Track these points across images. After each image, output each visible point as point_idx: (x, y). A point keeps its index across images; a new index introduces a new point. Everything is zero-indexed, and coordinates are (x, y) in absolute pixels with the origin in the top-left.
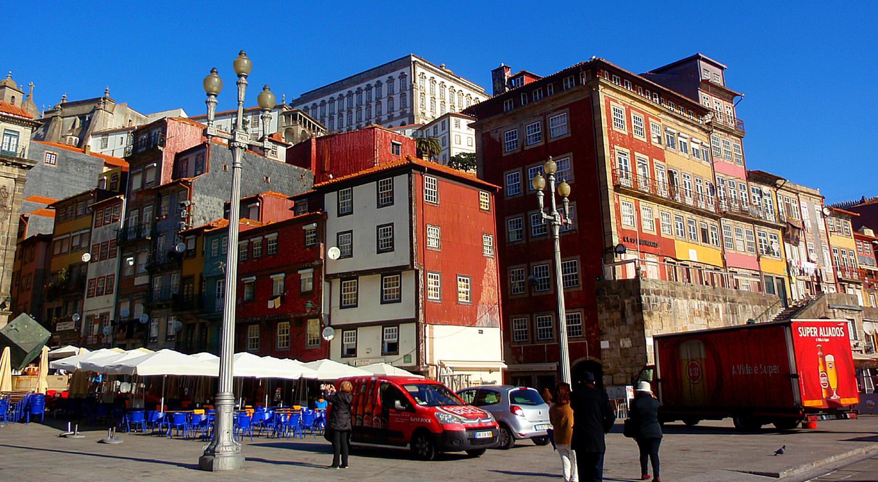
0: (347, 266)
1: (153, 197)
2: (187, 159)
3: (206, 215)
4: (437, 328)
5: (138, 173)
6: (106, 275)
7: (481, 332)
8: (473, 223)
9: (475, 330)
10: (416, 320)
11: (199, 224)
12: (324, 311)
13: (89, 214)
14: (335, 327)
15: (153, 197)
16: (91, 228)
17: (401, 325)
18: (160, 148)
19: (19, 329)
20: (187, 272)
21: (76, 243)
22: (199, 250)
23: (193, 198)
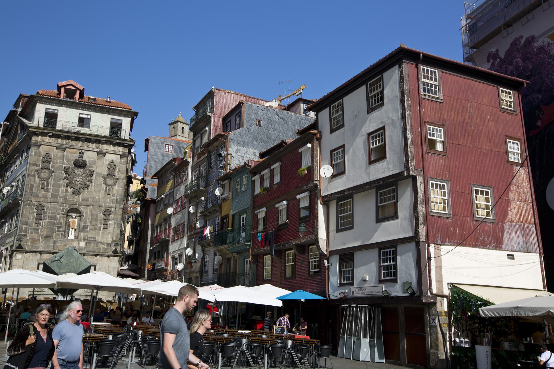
0: (340, 185)
1: (206, 155)
2: (230, 121)
4: (445, 249)
7: (511, 257)
8: (492, 124)
9: (505, 253)
10: (414, 239)
15: (206, 155)
16: (174, 189)
17: (400, 248)
18: (210, 114)
20: (224, 213)
23: (230, 149)
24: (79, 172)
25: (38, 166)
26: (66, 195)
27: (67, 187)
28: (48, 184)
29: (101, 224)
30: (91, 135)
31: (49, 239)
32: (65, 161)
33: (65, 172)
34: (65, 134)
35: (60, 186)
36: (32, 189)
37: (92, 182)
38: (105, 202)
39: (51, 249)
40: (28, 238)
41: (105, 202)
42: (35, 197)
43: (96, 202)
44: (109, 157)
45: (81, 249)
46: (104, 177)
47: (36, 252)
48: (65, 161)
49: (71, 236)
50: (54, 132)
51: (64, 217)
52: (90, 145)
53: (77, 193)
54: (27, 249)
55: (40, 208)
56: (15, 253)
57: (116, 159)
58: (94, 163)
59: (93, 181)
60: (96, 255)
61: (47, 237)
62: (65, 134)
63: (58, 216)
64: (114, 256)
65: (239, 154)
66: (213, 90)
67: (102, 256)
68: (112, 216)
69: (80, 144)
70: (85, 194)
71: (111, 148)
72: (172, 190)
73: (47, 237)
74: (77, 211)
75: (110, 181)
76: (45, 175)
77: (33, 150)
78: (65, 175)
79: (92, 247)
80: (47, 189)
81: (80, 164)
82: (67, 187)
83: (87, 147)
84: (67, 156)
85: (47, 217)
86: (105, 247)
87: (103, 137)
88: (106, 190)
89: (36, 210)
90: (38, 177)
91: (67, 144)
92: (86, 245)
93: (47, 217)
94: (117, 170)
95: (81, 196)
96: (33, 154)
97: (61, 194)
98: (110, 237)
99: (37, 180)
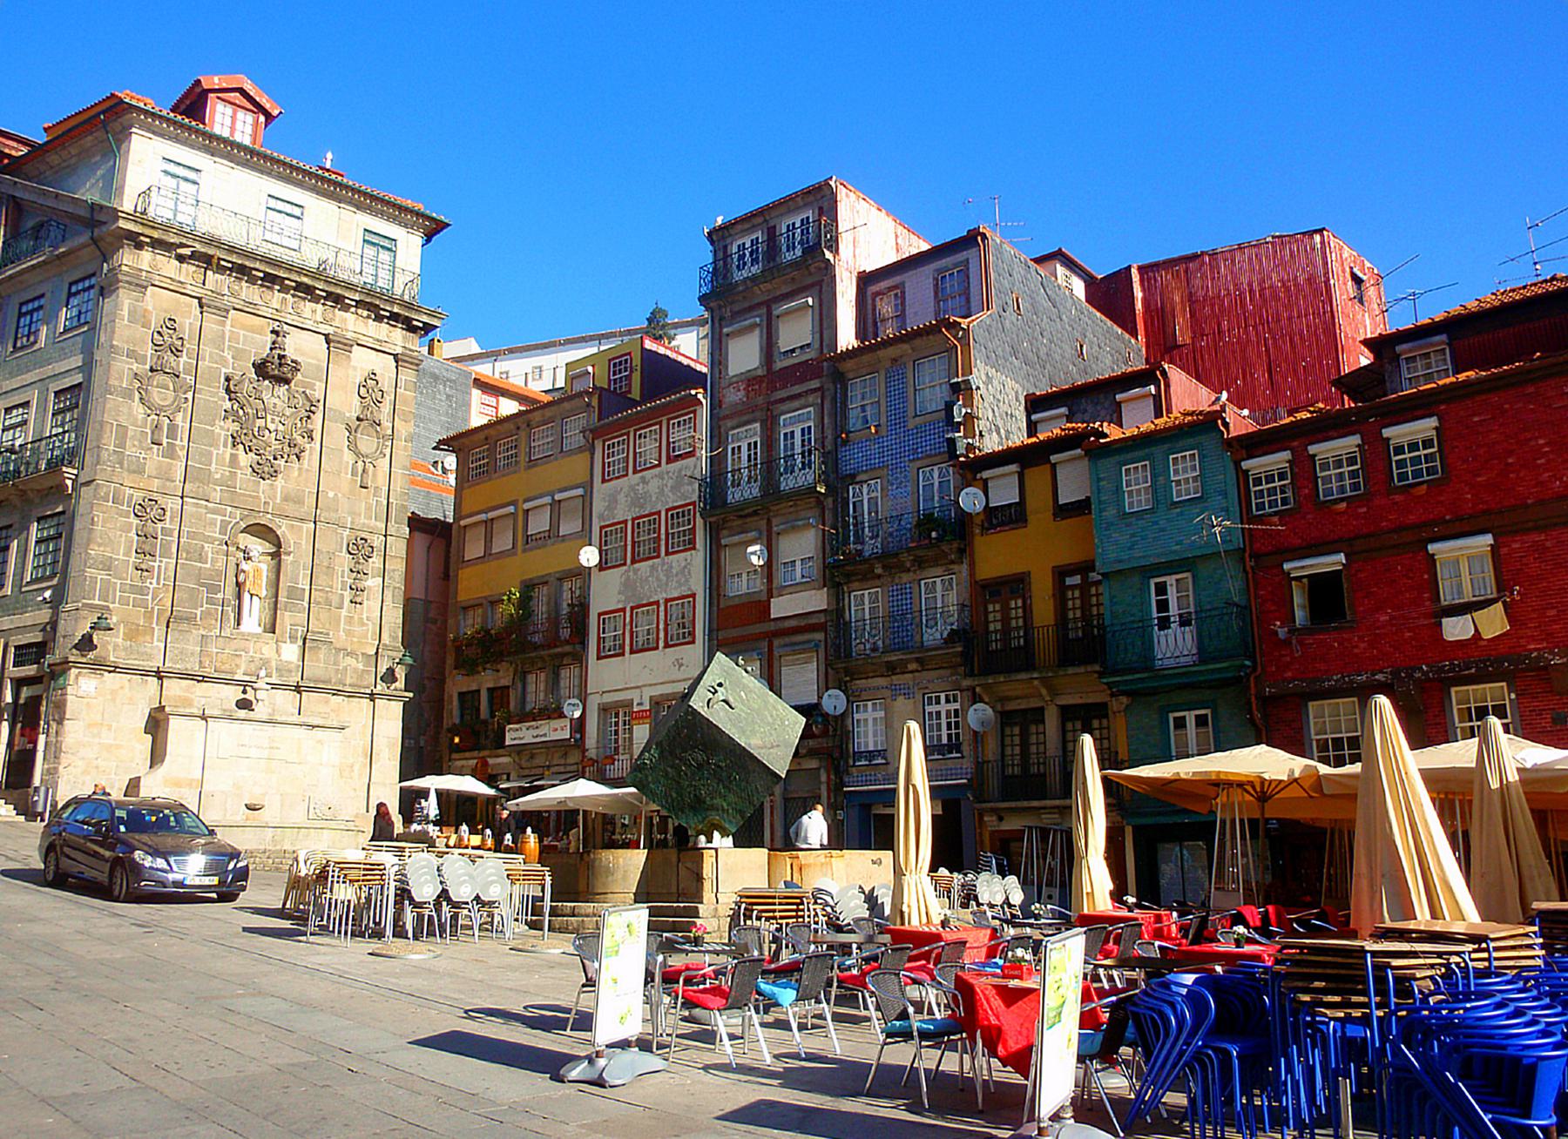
1: (815, 384)
2: (903, 284)
3: (1000, 423)
5: (755, 325)
6: (661, 597)
11: (991, 444)
13: (580, 450)
15: (815, 384)
21: (539, 523)
22: (1039, 504)
24: (275, 396)
25: (140, 359)
28: (173, 430)
31: (184, 626)
32: (228, 355)
33: (228, 391)
38: (354, 513)
39: (194, 668)
40: (115, 619)
41: (354, 513)
42: (131, 472)
43: (328, 509)
44: (363, 361)
47: (145, 673)
50: (198, 247)
52: (308, 307)
55: (147, 510)
56: (74, 671)
57: (384, 366)
59: (317, 436)
60: (337, 692)
64: (390, 697)
66: (832, 183)
67: (351, 695)
68: (376, 561)
69: (276, 298)
70: (294, 478)
74: (263, 531)
75: (367, 443)
76: (162, 394)
77: (125, 300)
78: (228, 405)
79: (318, 666)
81: (275, 370)
84: (234, 338)
87: (350, 287)
89: (136, 521)
94: (386, 408)
95: (280, 482)
96: (126, 313)
97: (218, 471)
98: (372, 628)
99: (139, 410)
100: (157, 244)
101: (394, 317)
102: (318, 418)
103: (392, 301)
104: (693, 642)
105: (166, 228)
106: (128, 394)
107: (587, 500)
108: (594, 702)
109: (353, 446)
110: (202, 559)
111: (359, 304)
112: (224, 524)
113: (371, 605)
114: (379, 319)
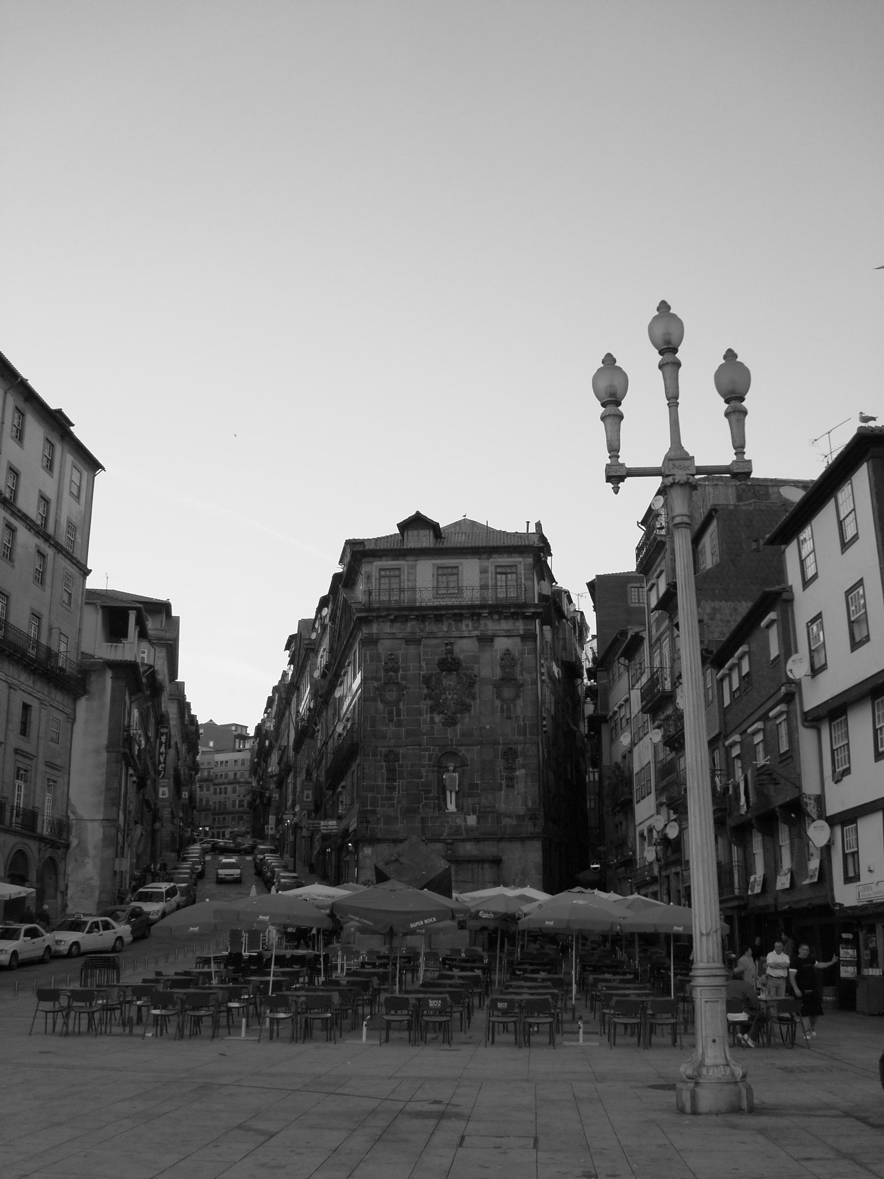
5: (653, 585)
12: (810, 787)
14: (832, 821)
18: (663, 539)
19: (403, 860)
24: (449, 680)
25: (377, 679)
26: (432, 728)
27: (432, 712)
29: (502, 779)
30: (461, 607)
32: (423, 664)
34: (415, 613)
35: (420, 712)
36: (373, 725)
37: (474, 698)
44: (502, 644)
45: (469, 830)
46: (494, 686)
48: (423, 664)
49: (452, 807)
50: (396, 613)
51: (433, 772)
53: (451, 722)
54: (379, 836)
55: (391, 757)
58: (476, 659)
59: (477, 695)
60: (500, 840)
61: (410, 812)
62: (415, 613)
63: (423, 770)
64: (532, 838)
65: (718, 616)
67: (512, 839)
68: (520, 760)
70: (466, 722)
71: (505, 625)
72: (627, 696)
73: (410, 812)
75: (508, 693)
76: (391, 696)
78: (425, 691)
80: (399, 721)
82: (432, 712)
83: (458, 629)
85: (405, 774)
86: (514, 823)
87: (482, 607)
88: (502, 711)
90: (382, 701)
91: (422, 631)
92: (478, 822)
93: (405, 774)
94: (518, 669)
97: (424, 728)
99: (381, 706)
100: (377, 617)
101: (513, 614)
102: (477, 686)
103: (509, 607)
104: (651, 793)
105: (378, 609)
106: (374, 700)
107: (627, 700)
108: (638, 829)
109: (499, 696)
110: (420, 777)
111: (489, 613)
112: (430, 756)
113: (520, 787)
114: (506, 618)
